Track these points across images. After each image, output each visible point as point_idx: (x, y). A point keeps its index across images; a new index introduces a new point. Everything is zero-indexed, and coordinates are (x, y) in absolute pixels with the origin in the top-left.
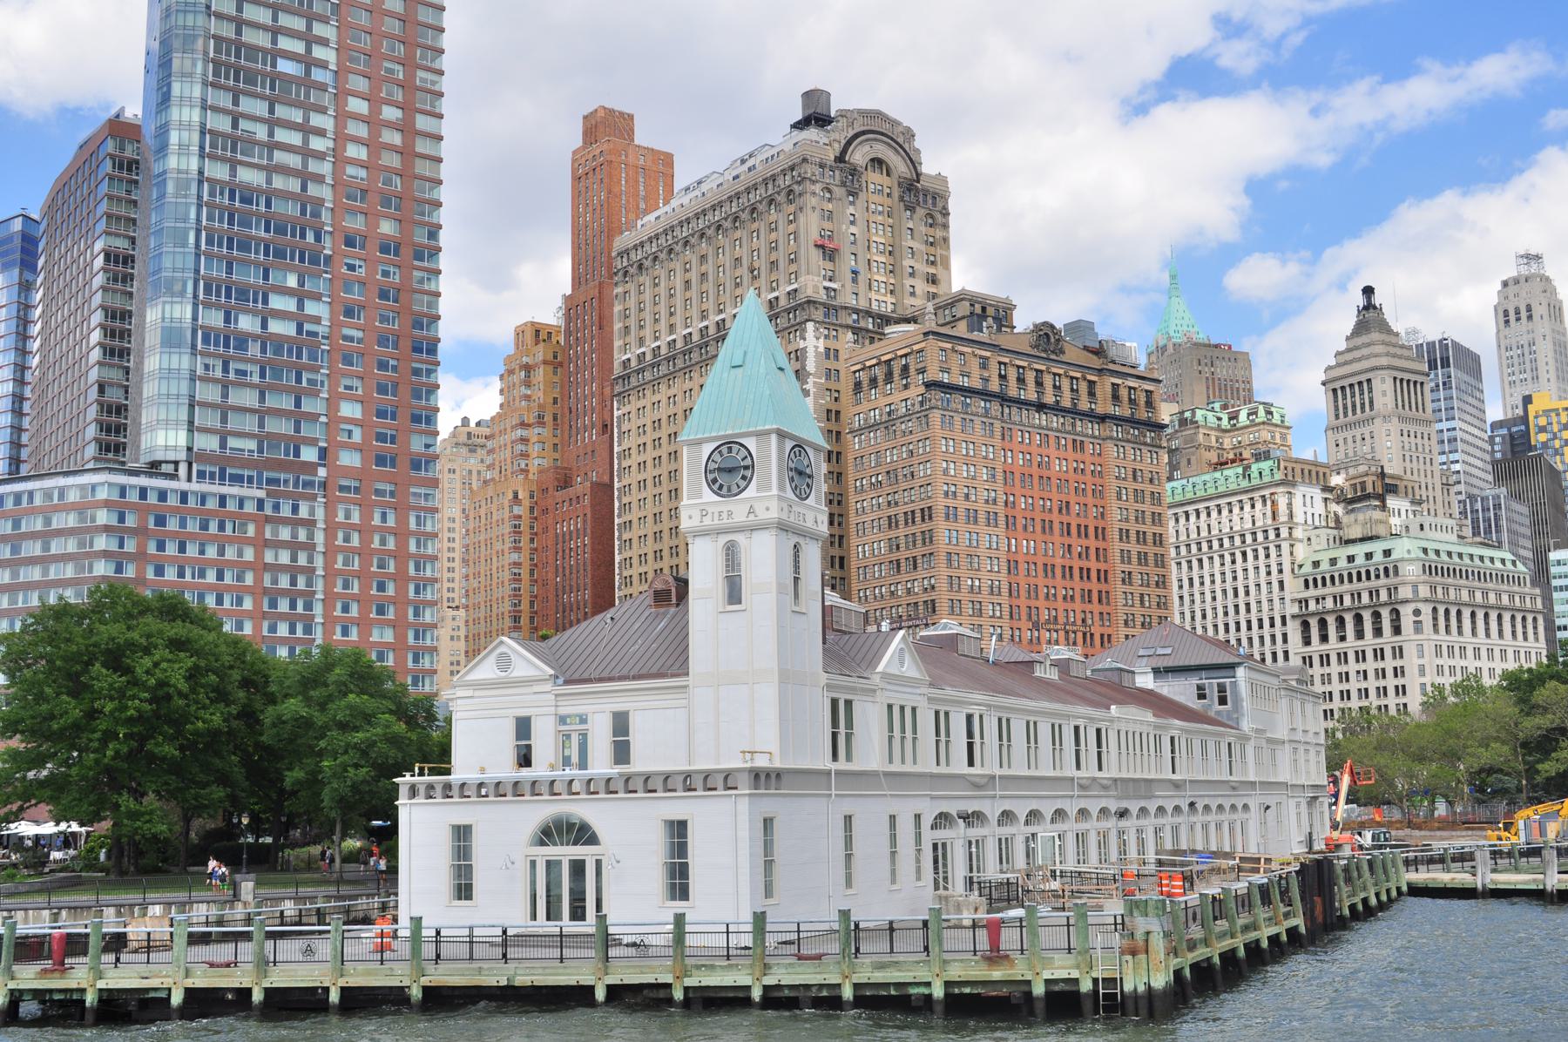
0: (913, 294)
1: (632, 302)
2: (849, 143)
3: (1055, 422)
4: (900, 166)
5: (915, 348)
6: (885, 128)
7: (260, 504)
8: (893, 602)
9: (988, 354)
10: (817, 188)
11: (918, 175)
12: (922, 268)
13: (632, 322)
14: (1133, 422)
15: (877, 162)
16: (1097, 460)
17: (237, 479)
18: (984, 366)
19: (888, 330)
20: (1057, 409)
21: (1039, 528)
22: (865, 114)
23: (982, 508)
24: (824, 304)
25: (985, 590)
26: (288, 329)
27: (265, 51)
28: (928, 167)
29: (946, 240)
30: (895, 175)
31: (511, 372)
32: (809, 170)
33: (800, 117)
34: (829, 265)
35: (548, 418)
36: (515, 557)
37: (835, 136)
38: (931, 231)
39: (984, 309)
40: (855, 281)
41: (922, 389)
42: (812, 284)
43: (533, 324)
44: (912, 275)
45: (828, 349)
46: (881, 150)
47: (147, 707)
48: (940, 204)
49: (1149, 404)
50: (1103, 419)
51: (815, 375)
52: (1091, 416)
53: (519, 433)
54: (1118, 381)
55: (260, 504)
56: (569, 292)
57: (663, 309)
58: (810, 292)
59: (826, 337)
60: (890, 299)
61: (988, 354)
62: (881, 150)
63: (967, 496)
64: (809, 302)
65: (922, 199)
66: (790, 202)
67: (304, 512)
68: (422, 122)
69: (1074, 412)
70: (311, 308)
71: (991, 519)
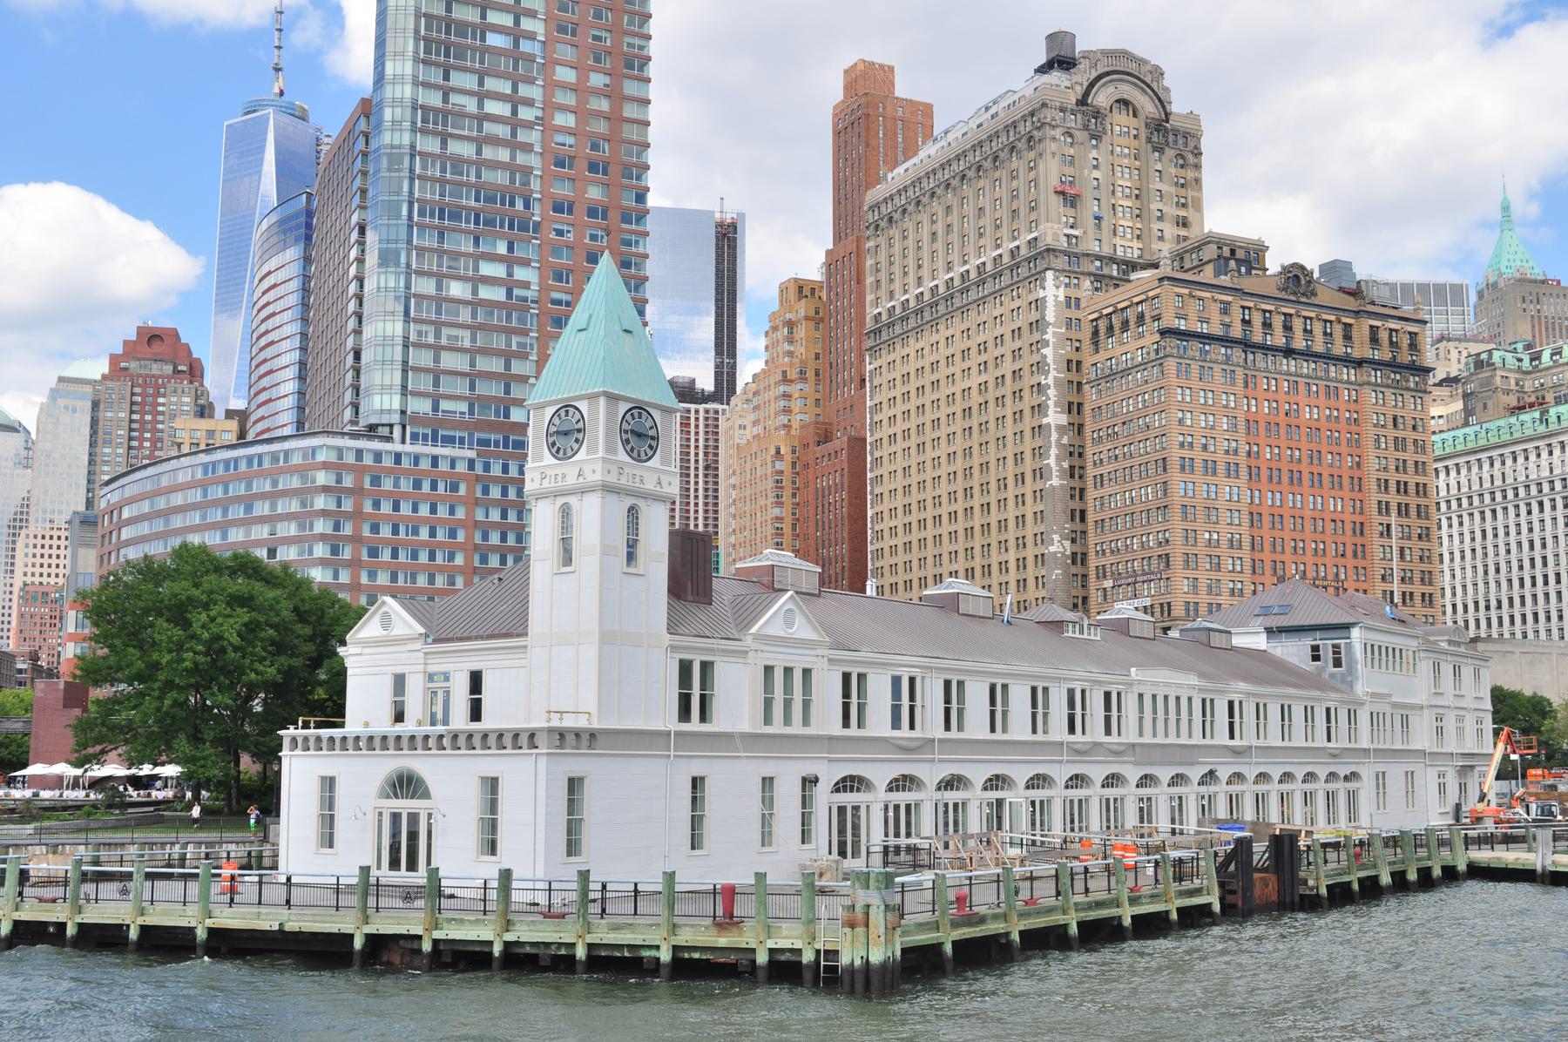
0: (1161, 238)
1: (883, 257)
2: (1092, 85)
3: (1306, 367)
4: (1148, 107)
5: (1151, 294)
6: (1132, 67)
7: (471, 463)
8: (1129, 556)
9: (1230, 299)
10: (1058, 133)
11: (1167, 115)
12: (1172, 211)
13: (883, 276)
14: (1393, 365)
15: (1124, 103)
16: (1353, 407)
17: (449, 440)
18: (1225, 311)
19: (1133, 276)
20: (1308, 355)
21: (1285, 479)
22: (1108, 53)
23: (1221, 458)
24: (1065, 253)
25: (1224, 544)
26: (498, 294)
27: (474, 26)
28: (1178, 107)
29: (1197, 181)
30: (1142, 117)
31: (775, 329)
32: (1048, 115)
33: (1043, 60)
34: (1071, 212)
35: (810, 374)
36: (777, 512)
37: (1078, 78)
38: (1182, 172)
39: (1233, 252)
40: (1099, 227)
41: (1157, 337)
42: (1053, 231)
43: (796, 280)
44: (1160, 219)
45: (1068, 298)
47: (201, 659)
48: (1191, 145)
49: (1414, 346)
50: (1359, 363)
51: (1054, 325)
52: (1347, 361)
53: (782, 388)
54: (1378, 323)
55: (471, 463)
56: (831, 247)
57: (911, 261)
58: (1049, 240)
59: (1067, 285)
60: (1136, 244)
61: (1230, 299)
62: (1128, 91)
63: (1205, 447)
64: (1048, 250)
65: (1172, 139)
66: (1031, 148)
68: (630, 88)
69: (1328, 358)
70: (520, 273)
71: (1232, 471)
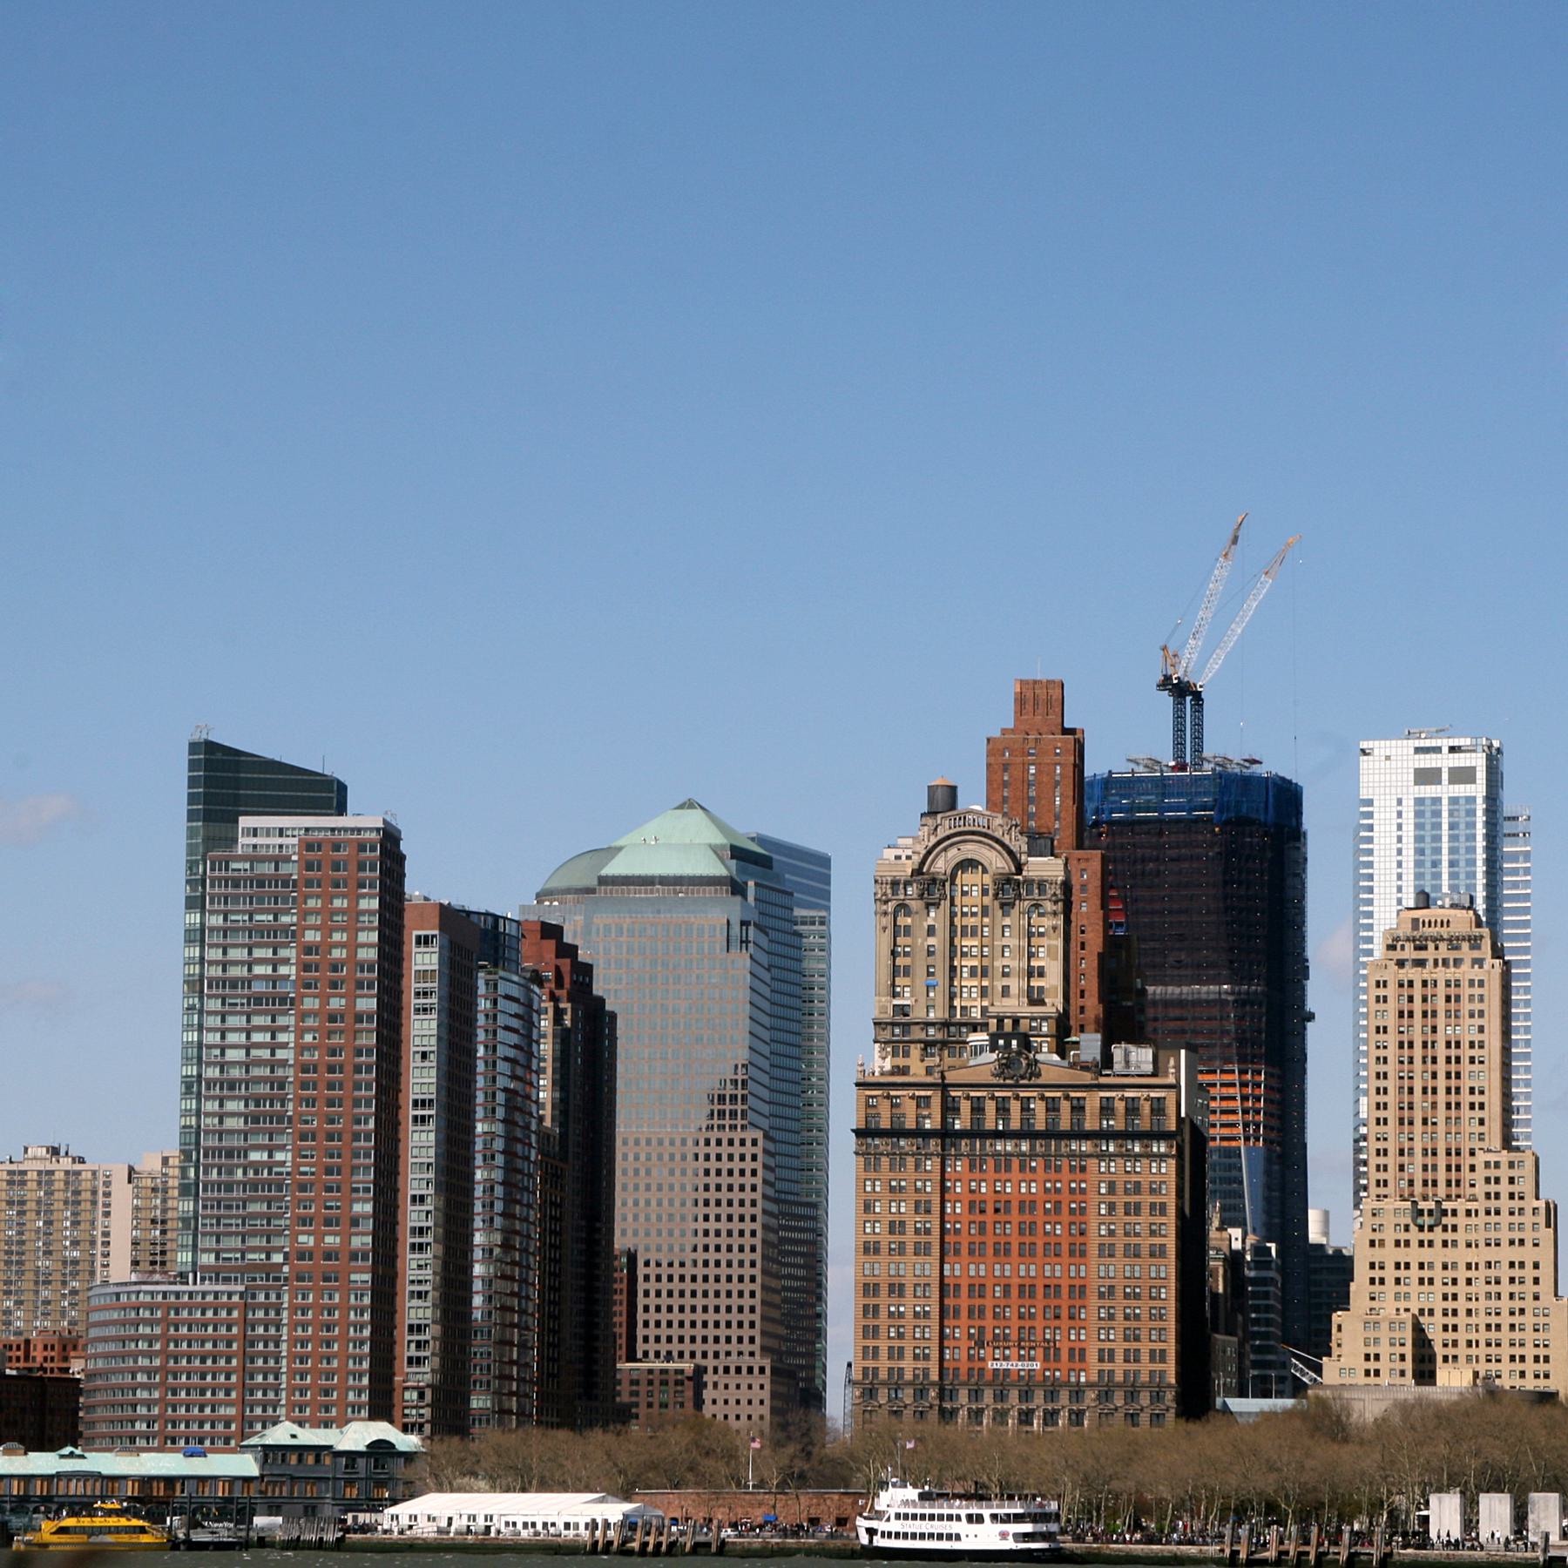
2: (929, 853)
4: (997, 862)
7: (242, 1295)
9: (929, 1093)
15: (968, 864)
17: (227, 1280)
21: (990, 1251)
27: (243, 980)
44: (1004, 975)
46: (971, 850)
55: (242, 1295)
61: (929, 1093)
62: (971, 850)
67: (273, 1298)
